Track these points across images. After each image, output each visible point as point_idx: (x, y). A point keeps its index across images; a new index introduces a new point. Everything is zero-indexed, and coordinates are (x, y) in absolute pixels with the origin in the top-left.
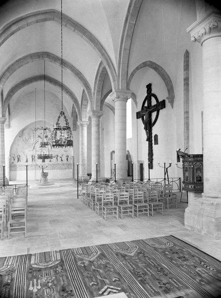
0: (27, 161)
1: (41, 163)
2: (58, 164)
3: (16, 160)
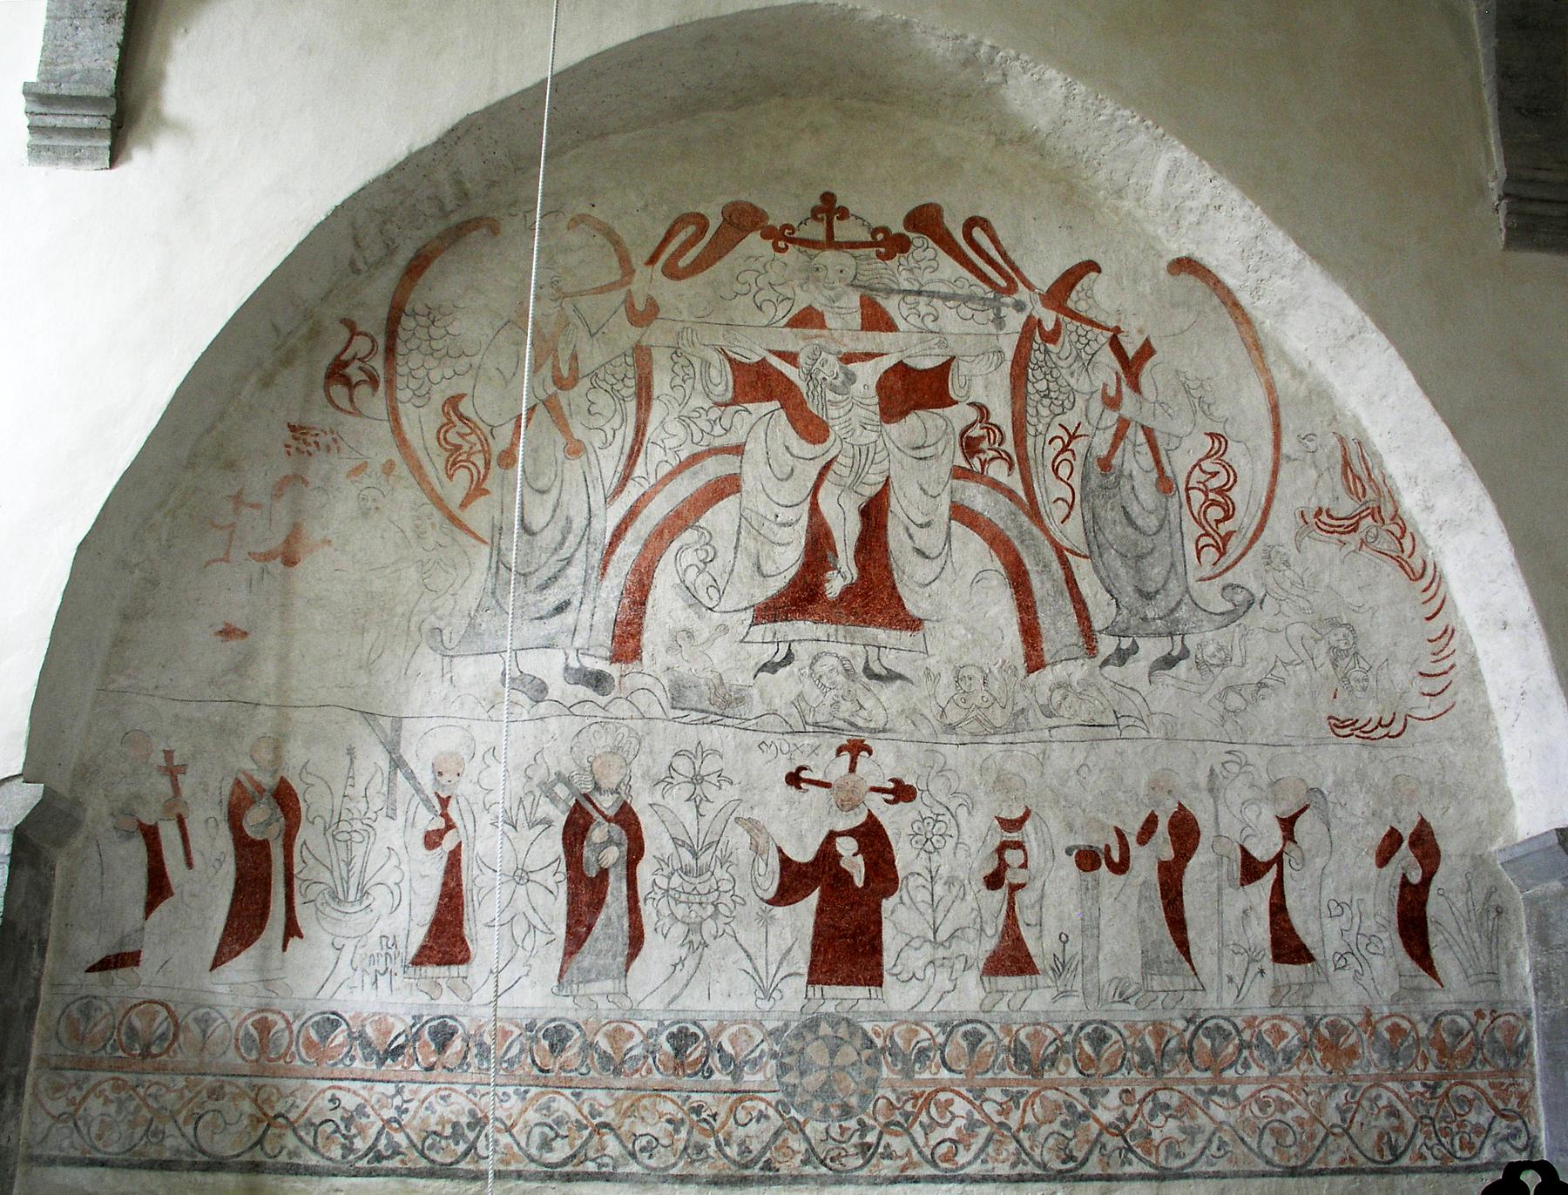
0: (446, 941)
1: (794, 996)
2: (1206, 1046)
3: (208, 886)
